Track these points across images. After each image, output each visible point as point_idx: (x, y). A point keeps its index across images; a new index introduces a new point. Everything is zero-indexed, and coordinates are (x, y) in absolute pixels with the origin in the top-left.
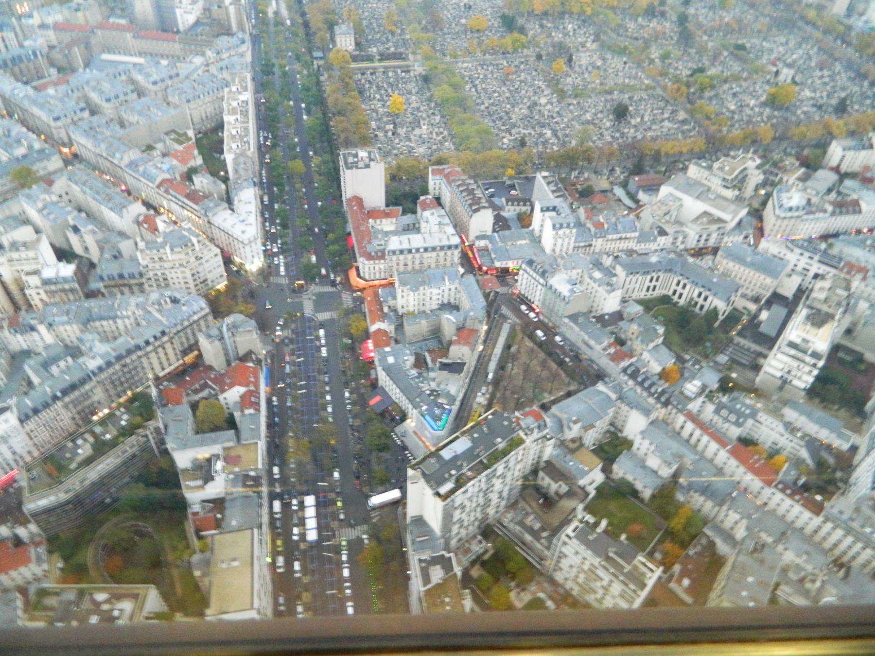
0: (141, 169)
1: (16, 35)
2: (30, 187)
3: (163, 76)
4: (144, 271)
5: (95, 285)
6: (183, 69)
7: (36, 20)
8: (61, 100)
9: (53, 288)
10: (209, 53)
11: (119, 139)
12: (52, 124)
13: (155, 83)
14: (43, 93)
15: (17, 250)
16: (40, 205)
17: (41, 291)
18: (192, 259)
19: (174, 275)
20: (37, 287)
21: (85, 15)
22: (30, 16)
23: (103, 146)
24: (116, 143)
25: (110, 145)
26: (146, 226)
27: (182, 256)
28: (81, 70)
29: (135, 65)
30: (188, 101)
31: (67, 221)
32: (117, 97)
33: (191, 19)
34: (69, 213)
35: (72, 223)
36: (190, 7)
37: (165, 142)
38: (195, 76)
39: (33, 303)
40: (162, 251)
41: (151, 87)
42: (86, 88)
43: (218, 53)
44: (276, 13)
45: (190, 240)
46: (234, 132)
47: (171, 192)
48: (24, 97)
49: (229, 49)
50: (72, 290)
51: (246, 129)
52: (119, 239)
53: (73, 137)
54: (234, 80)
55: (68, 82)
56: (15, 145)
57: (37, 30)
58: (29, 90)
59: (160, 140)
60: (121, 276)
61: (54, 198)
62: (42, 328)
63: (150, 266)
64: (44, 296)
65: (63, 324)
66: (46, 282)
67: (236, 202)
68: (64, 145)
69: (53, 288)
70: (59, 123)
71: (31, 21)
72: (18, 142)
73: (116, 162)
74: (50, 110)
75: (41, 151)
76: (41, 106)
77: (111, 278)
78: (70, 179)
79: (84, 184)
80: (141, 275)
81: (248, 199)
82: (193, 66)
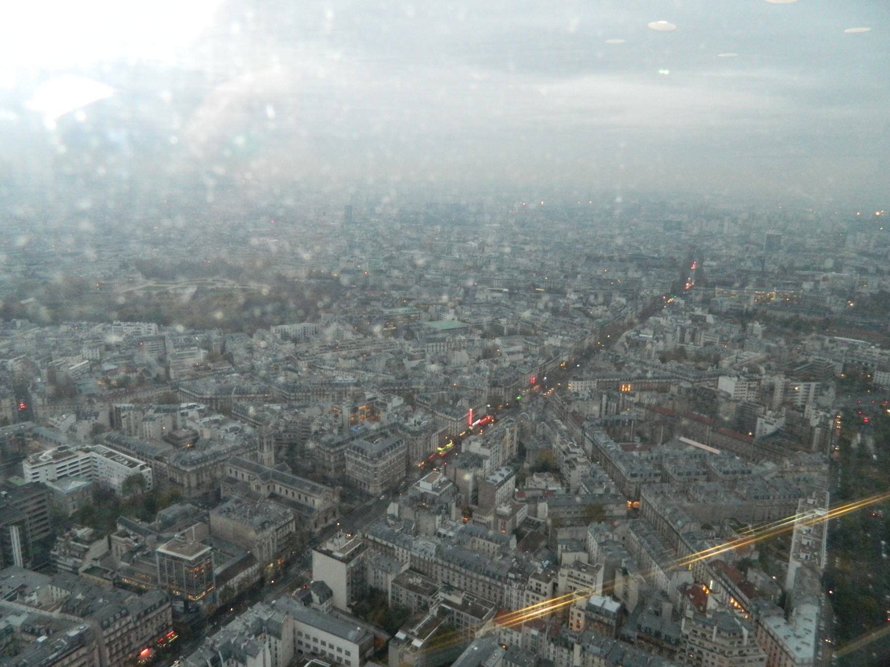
0: (699, 542)
1: (618, 406)
2: (600, 522)
3: (736, 469)
4: (682, 640)
5: (627, 631)
6: (756, 469)
7: (636, 399)
8: (641, 462)
9: (594, 616)
10: (787, 462)
11: (685, 509)
12: (628, 479)
13: (726, 473)
14: (629, 453)
15: (579, 569)
16: (603, 540)
17: (583, 614)
18: (736, 652)
19: (710, 659)
20: (580, 609)
21: (674, 405)
22: (633, 395)
23: (668, 511)
24: (681, 512)
25: (675, 511)
26: (691, 596)
27: (727, 644)
28: (659, 444)
29: (711, 453)
30: (757, 498)
31: (621, 561)
32: (689, 474)
33: (770, 429)
34: (624, 556)
35: (623, 565)
36: (773, 419)
37: (722, 528)
38: (767, 478)
39: (571, 621)
40: (708, 628)
41: (720, 475)
42: (664, 460)
43: (796, 465)
44: (862, 445)
45: (742, 631)
46: (805, 542)
47: (723, 574)
48: (613, 451)
49: (810, 464)
50: (608, 625)
51: (819, 544)
52: (660, 598)
53: (643, 494)
54: (810, 494)
55: (650, 450)
56: (597, 485)
57: (633, 406)
58: (620, 449)
59: (718, 524)
60: (658, 634)
61: (616, 539)
62: (577, 648)
63: (690, 638)
64: (582, 622)
65: (595, 655)
66: (591, 608)
67: (794, 613)
68: (629, 498)
69: (594, 616)
70: (634, 480)
71: (631, 399)
72: (601, 483)
73: (675, 527)
74: (632, 468)
75: (615, 496)
76: (625, 462)
77: (648, 631)
78: (632, 528)
79: (645, 536)
80: (678, 642)
81: (810, 614)
82: (762, 469)
